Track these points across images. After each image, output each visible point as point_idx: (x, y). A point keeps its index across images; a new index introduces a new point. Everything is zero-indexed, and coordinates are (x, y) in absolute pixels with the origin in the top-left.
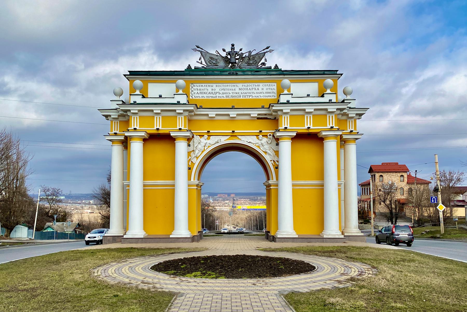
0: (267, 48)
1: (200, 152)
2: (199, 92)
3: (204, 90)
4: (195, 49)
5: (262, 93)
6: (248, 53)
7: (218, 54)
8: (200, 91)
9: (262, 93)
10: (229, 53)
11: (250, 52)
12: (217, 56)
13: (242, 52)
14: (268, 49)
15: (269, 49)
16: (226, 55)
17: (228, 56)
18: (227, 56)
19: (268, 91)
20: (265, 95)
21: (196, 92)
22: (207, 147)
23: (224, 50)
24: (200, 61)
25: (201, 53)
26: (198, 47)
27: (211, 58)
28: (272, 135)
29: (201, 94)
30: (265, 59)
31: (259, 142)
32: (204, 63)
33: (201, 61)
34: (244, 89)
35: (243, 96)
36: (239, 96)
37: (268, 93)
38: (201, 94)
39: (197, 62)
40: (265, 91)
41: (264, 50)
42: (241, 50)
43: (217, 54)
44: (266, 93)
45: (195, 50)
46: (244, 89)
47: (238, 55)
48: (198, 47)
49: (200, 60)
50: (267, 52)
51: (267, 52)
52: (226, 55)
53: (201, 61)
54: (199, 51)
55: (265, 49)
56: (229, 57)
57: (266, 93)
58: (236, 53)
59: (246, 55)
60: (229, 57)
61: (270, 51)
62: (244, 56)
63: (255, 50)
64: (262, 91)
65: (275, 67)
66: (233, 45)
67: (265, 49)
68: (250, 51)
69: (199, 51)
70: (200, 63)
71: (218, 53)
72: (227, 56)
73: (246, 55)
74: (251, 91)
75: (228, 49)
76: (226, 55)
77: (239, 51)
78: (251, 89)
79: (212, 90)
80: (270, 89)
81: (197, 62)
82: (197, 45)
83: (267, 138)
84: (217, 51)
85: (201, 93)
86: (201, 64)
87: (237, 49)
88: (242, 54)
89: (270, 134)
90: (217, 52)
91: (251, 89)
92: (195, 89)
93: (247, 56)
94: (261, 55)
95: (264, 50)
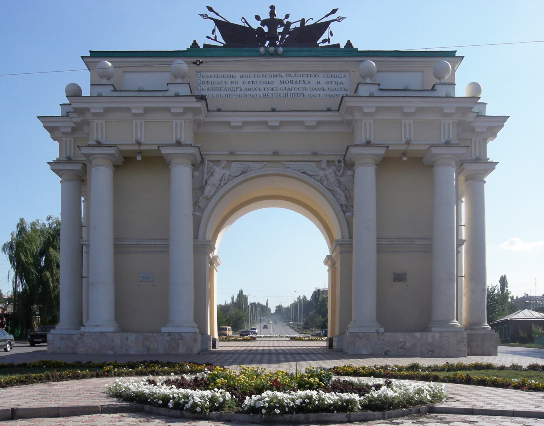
1: (213, 189)
4: (206, 14)
5: (322, 89)
6: (300, 22)
8: (213, 86)
10: (264, 23)
11: (303, 21)
12: (244, 27)
13: (289, 20)
18: (262, 27)
22: (226, 181)
24: (213, 37)
26: (210, 9)
29: (214, 90)
30: (329, 32)
32: (220, 38)
33: (216, 36)
35: (292, 94)
38: (214, 90)
41: (327, 16)
42: (287, 16)
43: (243, 24)
45: (205, 17)
49: (213, 33)
52: (260, 26)
53: (216, 36)
54: (211, 19)
57: (329, 89)
58: (280, 22)
60: (266, 29)
61: (339, 19)
62: (292, 26)
69: (211, 19)
70: (212, 39)
71: (246, 22)
72: (262, 27)
75: (265, 16)
76: (260, 26)
84: (243, 18)
86: (215, 40)
88: (289, 24)
90: (244, 21)
92: (204, 83)
94: (322, 27)
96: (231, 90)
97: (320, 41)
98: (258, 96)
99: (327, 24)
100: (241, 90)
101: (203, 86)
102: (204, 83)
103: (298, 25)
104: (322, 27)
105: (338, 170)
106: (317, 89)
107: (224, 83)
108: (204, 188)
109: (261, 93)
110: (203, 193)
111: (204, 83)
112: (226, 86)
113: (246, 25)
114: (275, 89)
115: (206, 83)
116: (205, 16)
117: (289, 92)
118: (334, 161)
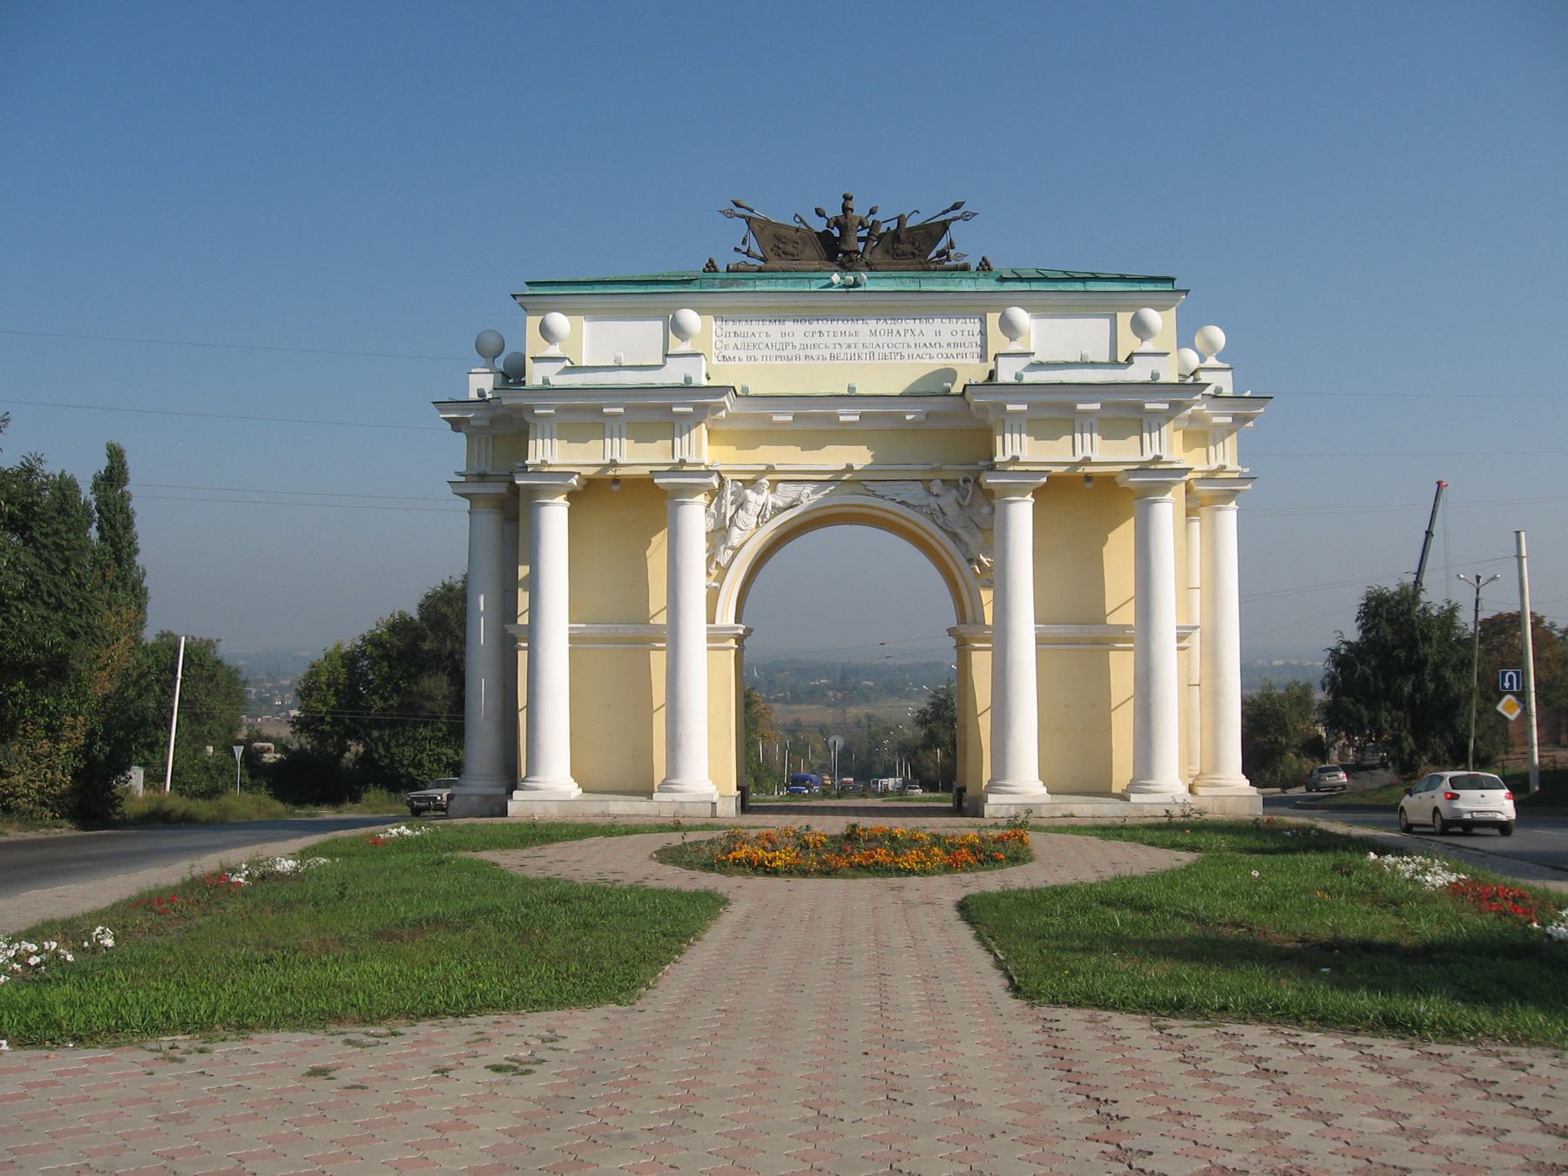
0: (956, 207)
2: (739, 341)
3: (757, 335)
5: (938, 345)
7: (803, 226)
8: (746, 340)
9: (938, 345)
11: (901, 220)
12: (797, 230)
14: (957, 209)
15: (962, 210)
16: (828, 226)
17: (832, 231)
19: (959, 339)
20: (945, 350)
21: (732, 341)
23: (819, 213)
25: (749, 220)
26: (737, 205)
27: (777, 237)
28: (972, 481)
31: (932, 501)
32: (756, 250)
34: (882, 332)
36: (868, 355)
37: (956, 345)
39: (737, 250)
40: (944, 340)
41: (945, 212)
42: (872, 212)
43: (797, 225)
44: (949, 345)
45: (730, 214)
46: (882, 332)
47: (864, 228)
48: (737, 205)
49: (744, 242)
50: (955, 219)
51: (955, 219)
53: (749, 247)
54: (742, 217)
55: (948, 211)
56: (836, 232)
59: (889, 229)
60: (836, 232)
61: (966, 217)
62: (883, 229)
63: (918, 213)
64: (938, 339)
65: (980, 264)
66: (847, 198)
67: (948, 211)
68: (901, 216)
69: (742, 217)
73: (889, 229)
74: (902, 339)
75: (834, 211)
77: (868, 216)
78: (902, 333)
79: (783, 335)
80: (966, 333)
81: (737, 250)
82: (736, 199)
83: (958, 490)
84: (796, 215)
85: (747, 347)
86: (747, 253)
87: (860, 210)
89: (965, 475)
90: (798, 220)
91: (902, 333)
93: (891, 229)
95: (945, 212)
96: (778, 347)
97: (933, 254)
98: (821, 357)
99: (945, 226)
100: (794, 347)
101: (726, 341)
102: (728, 334)
103: (893, 226)
104: (935, 231)
105: (962, 496)
106: (928, 345)
107: (763, 335)
108: (727, 531)
109: (827, 354)
110: (725, 539)
111: (728, 334)
112: (769, 340)
113: (803, 226)
114: (853, 346)
115: (732, 335)
116: (730, 214)
117: (877, 351)
118: (958, 481)
